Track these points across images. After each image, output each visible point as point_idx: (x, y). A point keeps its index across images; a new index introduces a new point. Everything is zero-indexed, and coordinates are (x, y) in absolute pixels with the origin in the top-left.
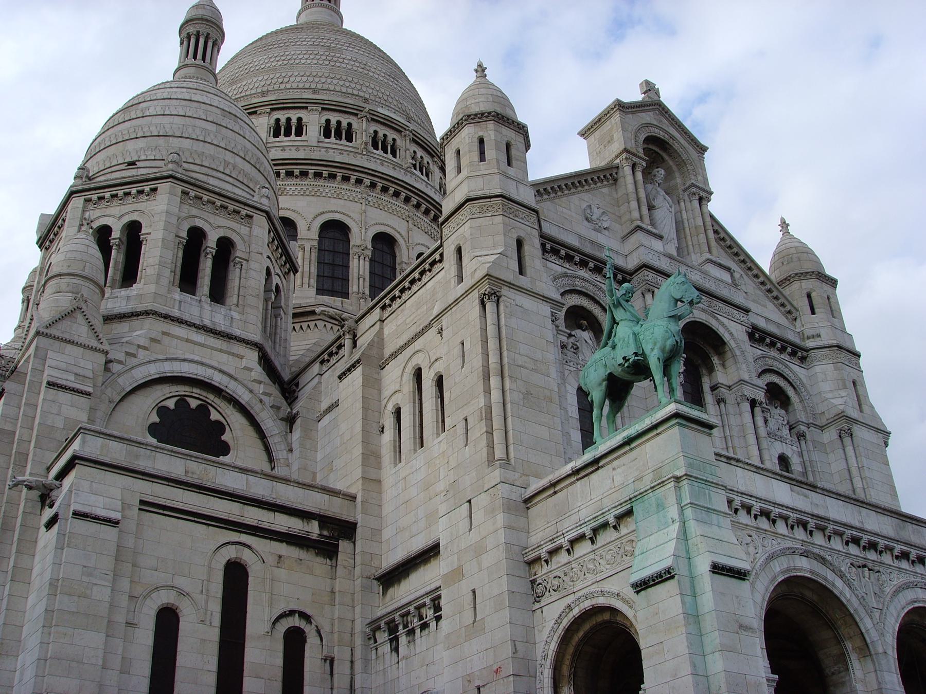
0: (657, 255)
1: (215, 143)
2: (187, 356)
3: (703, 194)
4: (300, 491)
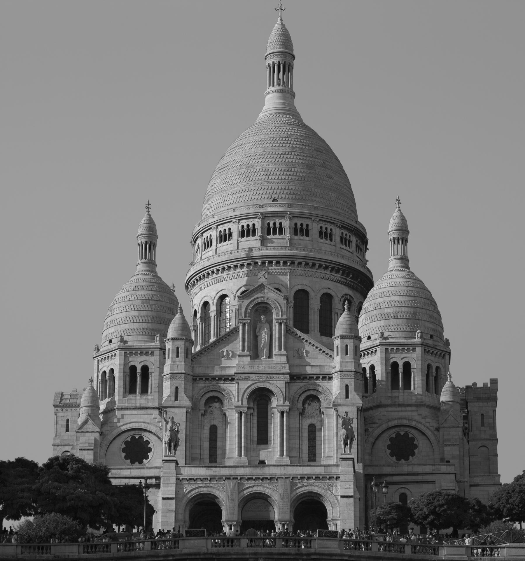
0: (243, 366)
1: (138, 321)
3: (281, 321)
4: (148, 470)
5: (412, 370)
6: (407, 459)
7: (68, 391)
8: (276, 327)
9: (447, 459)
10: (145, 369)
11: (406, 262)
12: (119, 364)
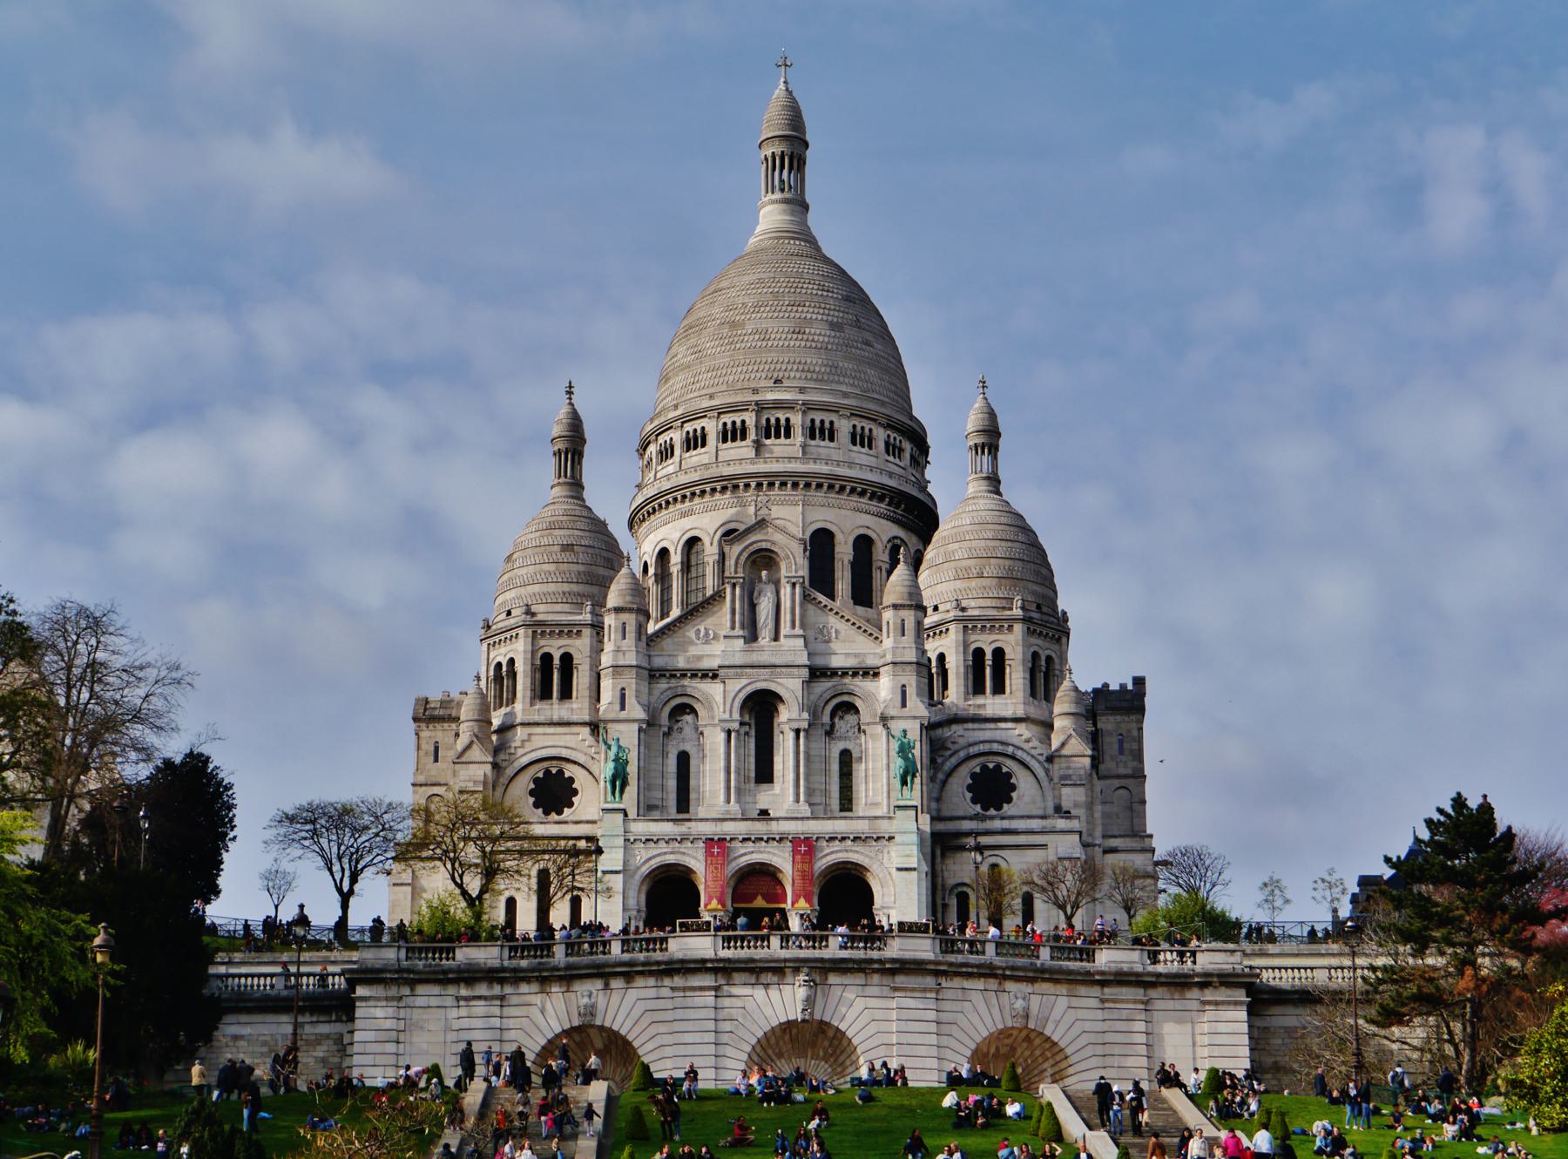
1: (555, 580)
2: (545, 745)
3: (794, 580)
5: (1007, 662)
6: (999, 808)
7: (435, 696)
8: (786, 591)
9: (1065, 809)
10: (567, 659)
11: (996, 484)
12: (525, 651)
